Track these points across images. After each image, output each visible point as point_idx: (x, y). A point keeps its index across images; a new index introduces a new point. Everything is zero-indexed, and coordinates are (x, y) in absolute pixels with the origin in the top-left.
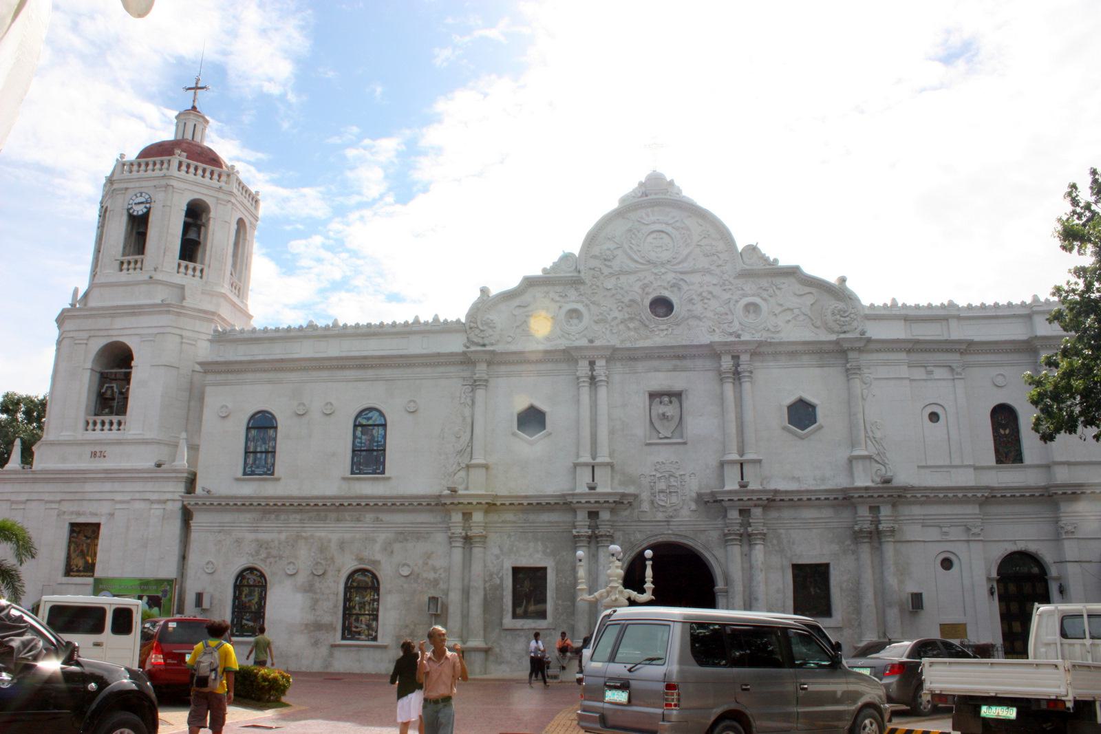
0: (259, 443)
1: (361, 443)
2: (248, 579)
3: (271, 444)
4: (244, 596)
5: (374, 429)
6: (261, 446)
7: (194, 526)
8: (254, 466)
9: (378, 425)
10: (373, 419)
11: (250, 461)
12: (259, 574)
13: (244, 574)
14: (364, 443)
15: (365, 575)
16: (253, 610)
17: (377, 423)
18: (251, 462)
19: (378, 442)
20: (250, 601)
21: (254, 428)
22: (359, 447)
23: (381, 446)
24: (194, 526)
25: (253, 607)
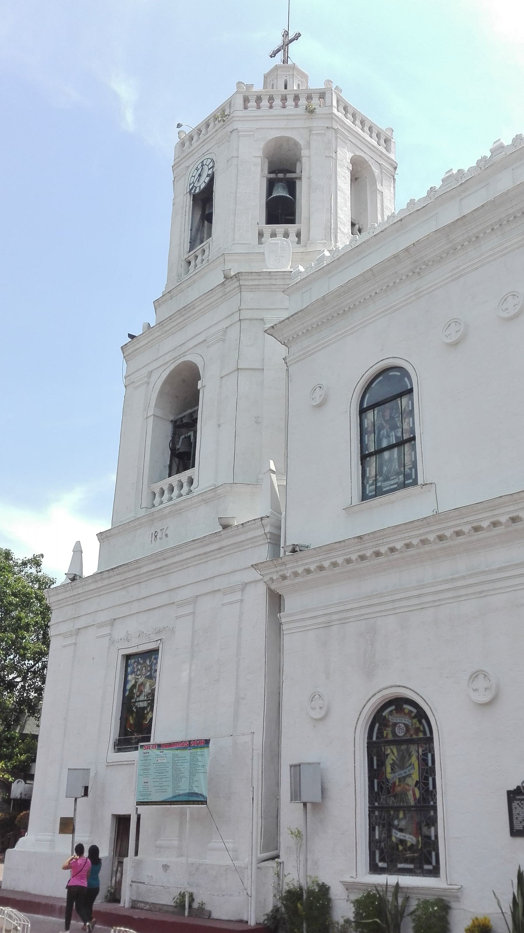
2: (395, 724)
3: (405, 426)
4: (389, 769)
6: (388, 436)
7: (287, 622)
8: (380, 478)
11: (371, 471)
12: (414, 711)
13: (385, 713)
16: (412, 803)
18: (373, 473)
20: (402, 780)
21: (372, 407)
24: (287, 622)
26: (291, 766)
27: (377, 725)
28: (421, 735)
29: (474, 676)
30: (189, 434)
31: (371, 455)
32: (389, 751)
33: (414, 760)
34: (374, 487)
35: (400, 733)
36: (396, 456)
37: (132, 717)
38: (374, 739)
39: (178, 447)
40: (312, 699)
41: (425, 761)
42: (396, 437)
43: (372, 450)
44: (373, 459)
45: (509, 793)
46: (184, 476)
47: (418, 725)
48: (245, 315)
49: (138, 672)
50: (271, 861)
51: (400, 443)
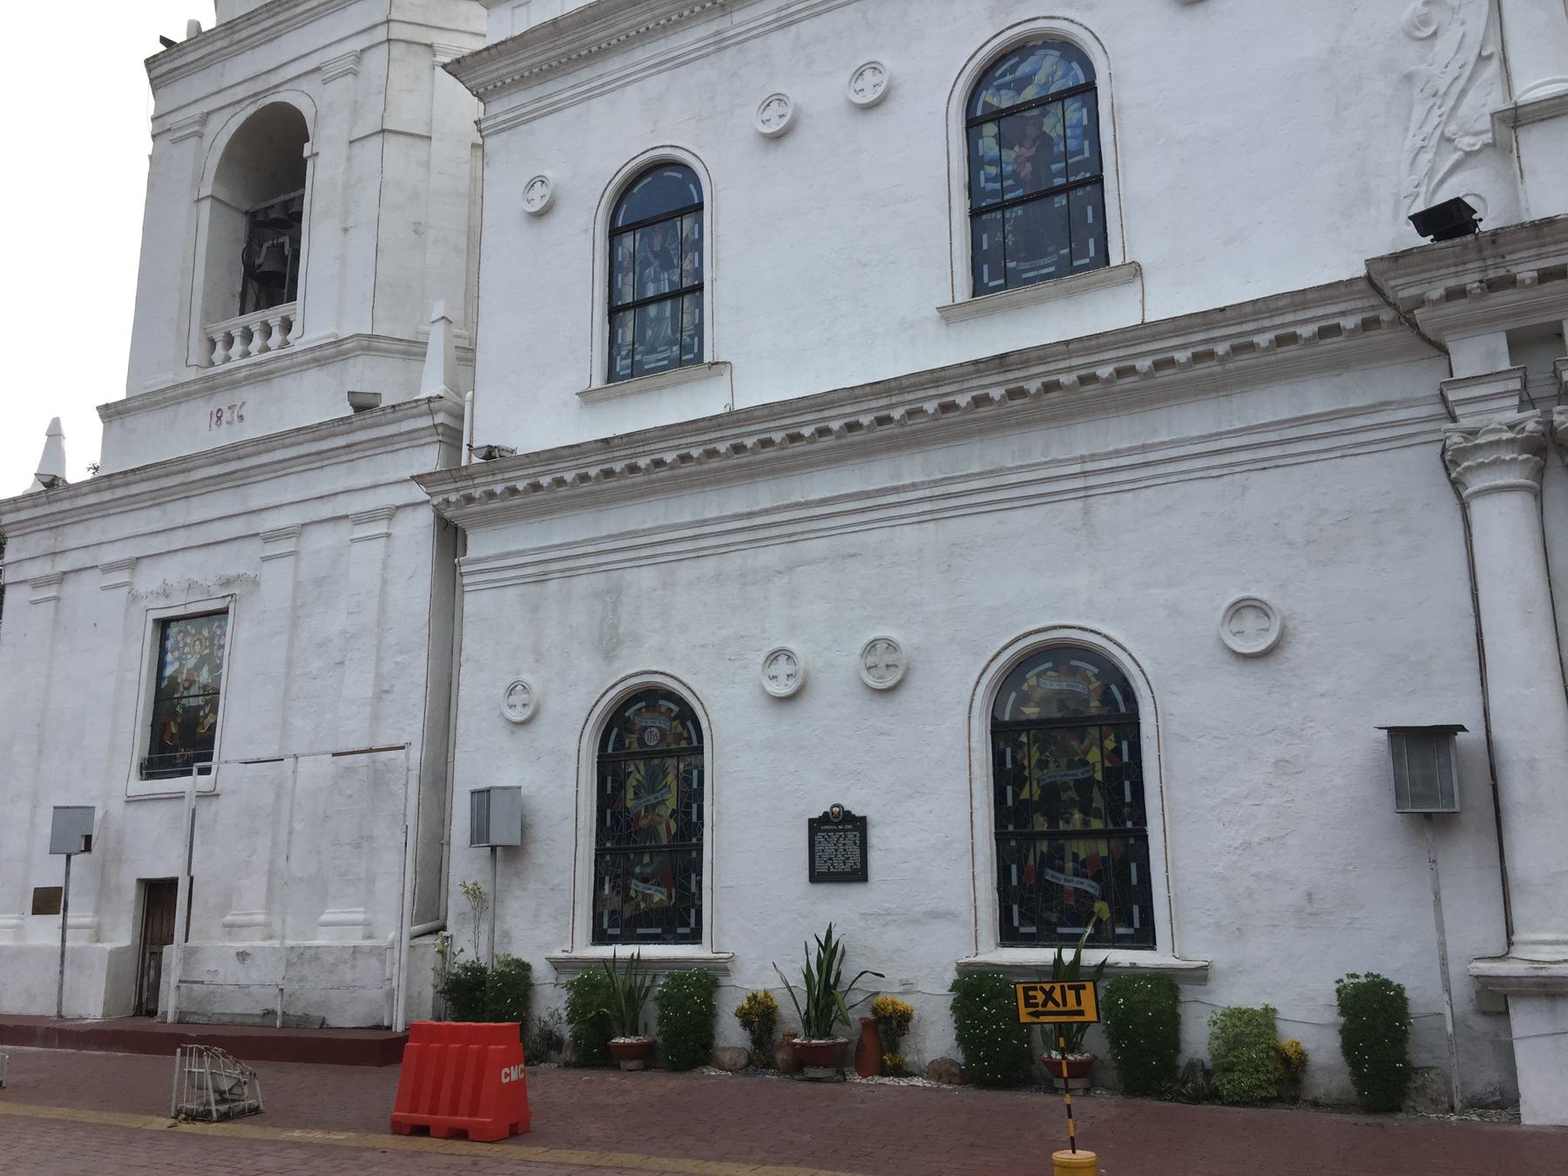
0: (650, 272)
1: (1001, 177)
2: (644, 729)
3: (687, 266)
4: (630, 794)
5: (1045, 114)
6: (657, 280)
8: (640, 349)
9: (1061, 97)
10: (1040, 77)
11: (627, 334)
14: (1015, 175)
15: (1074, 671)
17: (1053, 89)
18: (629, 338)
19: (1066, 155)
20: (651, 808)
21: (631, 227)
22: (993, 193)
23: (1080, 166)
25: (662, 829)
26: (473, 793)
27: (615, 731)
28: (684, 744)
29: (774, 657)
30: (281, 240)
31: (626, 307)
32: (632, 768)
33: (671, 779)
34: (629, 361)
35: (652, 740)
36: (668, 313)
37: (176, 722)
38: (610, 750)
39: (258, 262)
40: (511, 690)
41: (688, 781)
42: (671, 282)
43: (629, 299)
44: (630, 315)
45: (811, 821)
46: (274, 315)
47: (680, 729)
48: (397, 31)
49: (187, 650)
50: (429, 936)
51: (676, 294)
